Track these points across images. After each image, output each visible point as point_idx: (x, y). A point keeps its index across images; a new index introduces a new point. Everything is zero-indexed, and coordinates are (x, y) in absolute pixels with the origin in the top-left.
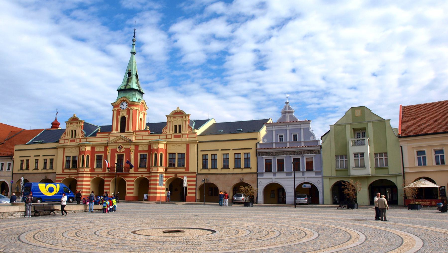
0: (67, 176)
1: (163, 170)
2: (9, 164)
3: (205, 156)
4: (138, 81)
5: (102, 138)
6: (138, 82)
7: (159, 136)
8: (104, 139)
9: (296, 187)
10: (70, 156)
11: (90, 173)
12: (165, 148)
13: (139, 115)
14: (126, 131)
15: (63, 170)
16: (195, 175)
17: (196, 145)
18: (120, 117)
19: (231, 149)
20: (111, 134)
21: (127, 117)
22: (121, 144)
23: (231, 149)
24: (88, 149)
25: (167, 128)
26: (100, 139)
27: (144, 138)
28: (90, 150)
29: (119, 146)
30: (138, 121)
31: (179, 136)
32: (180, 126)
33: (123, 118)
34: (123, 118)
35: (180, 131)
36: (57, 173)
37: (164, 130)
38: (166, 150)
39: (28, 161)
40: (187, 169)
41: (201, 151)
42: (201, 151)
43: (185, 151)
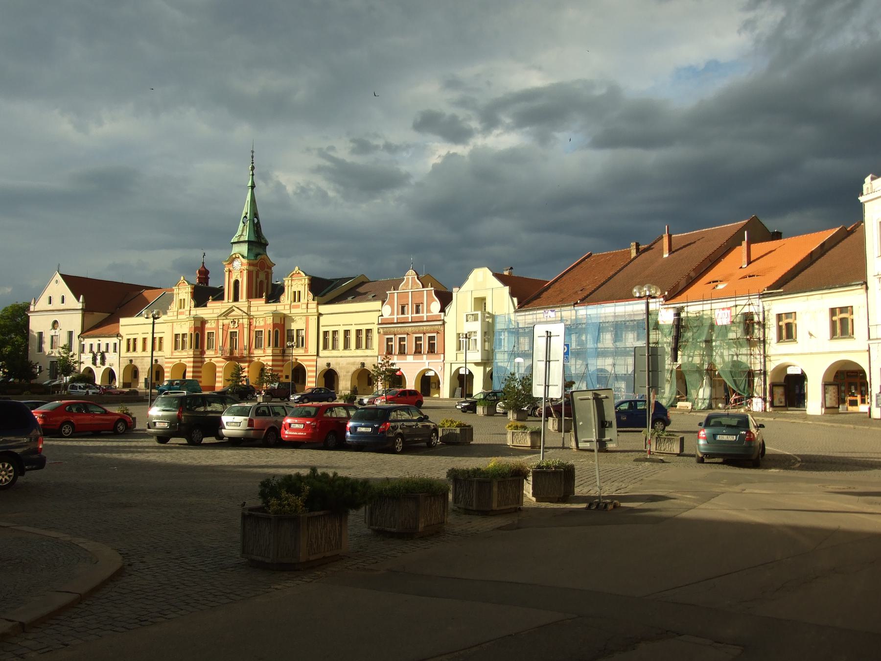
0: (177, 361)
1: (279, 352)
2: (115, 344)
3: (326, 333)
4: (257, 228)
5: (213, 309)
6: (259, 229)
7: (276, 306)
8: (215, 311)
9: (452, 373)
10: (179, 334)
11: (200, 356)
12: (282, 323)
13: (257, 276)
14: (240, 300)
15: (172, 352)
16: (315, 357)
17: (316, 317)
18: (232, 281)
19: (353, 324)
20: (223, 304)
21: (240, 280)
22: (232, 318)
23: (353, 325)
24: (199, 325)
25: (285, 296)
26: (211, 311)
27: (260, 309)
28: (200, 326)
29: (232, 320)
30: (256, 285)
31: (298, 307)
32: (299, 292)
33: (237, 283)
34: (237, 283)
35: (299, 301)
36: (166, 357)
37: (282, 298)
38: (284, 325)
39: (135, 340)
40: (306, 350)
41: (322, 326)
42: (322, 326)
43: (303, 327)
